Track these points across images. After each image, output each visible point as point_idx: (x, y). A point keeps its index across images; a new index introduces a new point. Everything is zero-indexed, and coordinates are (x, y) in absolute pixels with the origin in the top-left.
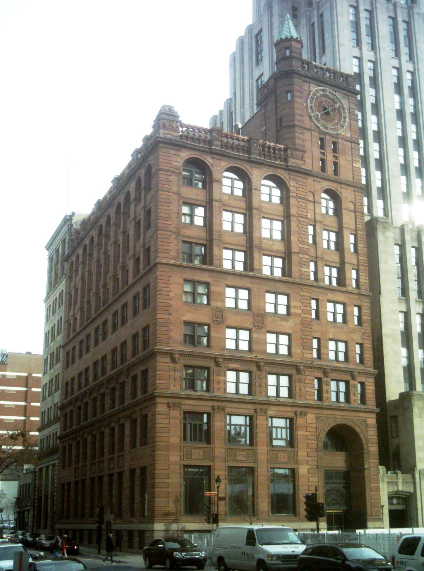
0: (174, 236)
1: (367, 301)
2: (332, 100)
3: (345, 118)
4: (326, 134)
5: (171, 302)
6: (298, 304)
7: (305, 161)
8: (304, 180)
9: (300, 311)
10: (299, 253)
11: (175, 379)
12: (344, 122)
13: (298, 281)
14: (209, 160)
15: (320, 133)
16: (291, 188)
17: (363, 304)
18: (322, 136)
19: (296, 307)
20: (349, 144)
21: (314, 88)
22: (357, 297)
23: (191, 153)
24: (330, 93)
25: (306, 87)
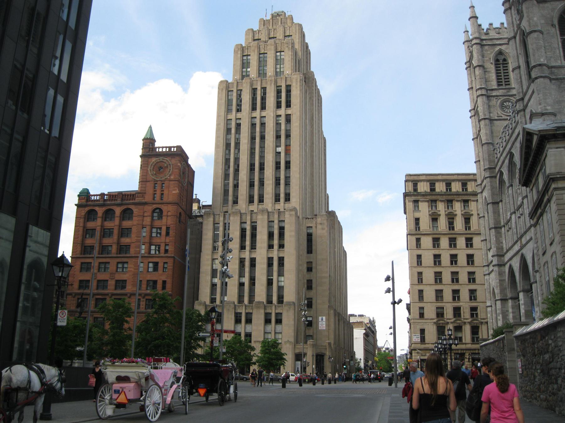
0: (79, 245)
1: (171, 259)
2: (165, 163)
3: (170, 170)
4: (157, 181)
5: (75, 273)
6: (133, 266)
7: (145, 198)
8: (143, 207)
9: (132, 269)
10: (136, 242)
11: (73, 304)
12: (169, 172)
13: (133, 255)
14: (97, 209)
15: (154, 181)
16: (135, 212)
17: (169, 261)
18: (156, 182)
19: (130, 268)
20: (172, 182)
21: (154, 160)
22: (166, 258)
23: (89, 207)
24: (163, 159)
25: (150, 160)
